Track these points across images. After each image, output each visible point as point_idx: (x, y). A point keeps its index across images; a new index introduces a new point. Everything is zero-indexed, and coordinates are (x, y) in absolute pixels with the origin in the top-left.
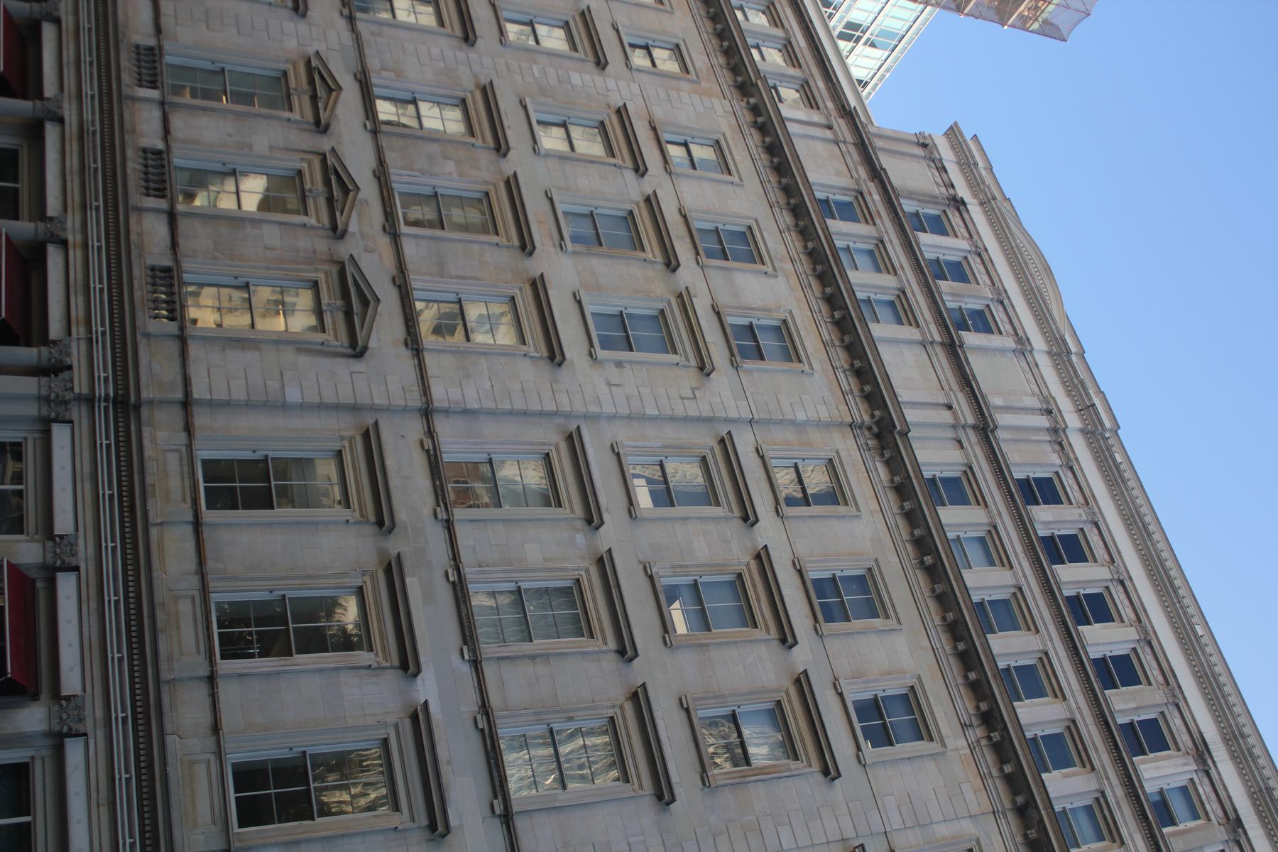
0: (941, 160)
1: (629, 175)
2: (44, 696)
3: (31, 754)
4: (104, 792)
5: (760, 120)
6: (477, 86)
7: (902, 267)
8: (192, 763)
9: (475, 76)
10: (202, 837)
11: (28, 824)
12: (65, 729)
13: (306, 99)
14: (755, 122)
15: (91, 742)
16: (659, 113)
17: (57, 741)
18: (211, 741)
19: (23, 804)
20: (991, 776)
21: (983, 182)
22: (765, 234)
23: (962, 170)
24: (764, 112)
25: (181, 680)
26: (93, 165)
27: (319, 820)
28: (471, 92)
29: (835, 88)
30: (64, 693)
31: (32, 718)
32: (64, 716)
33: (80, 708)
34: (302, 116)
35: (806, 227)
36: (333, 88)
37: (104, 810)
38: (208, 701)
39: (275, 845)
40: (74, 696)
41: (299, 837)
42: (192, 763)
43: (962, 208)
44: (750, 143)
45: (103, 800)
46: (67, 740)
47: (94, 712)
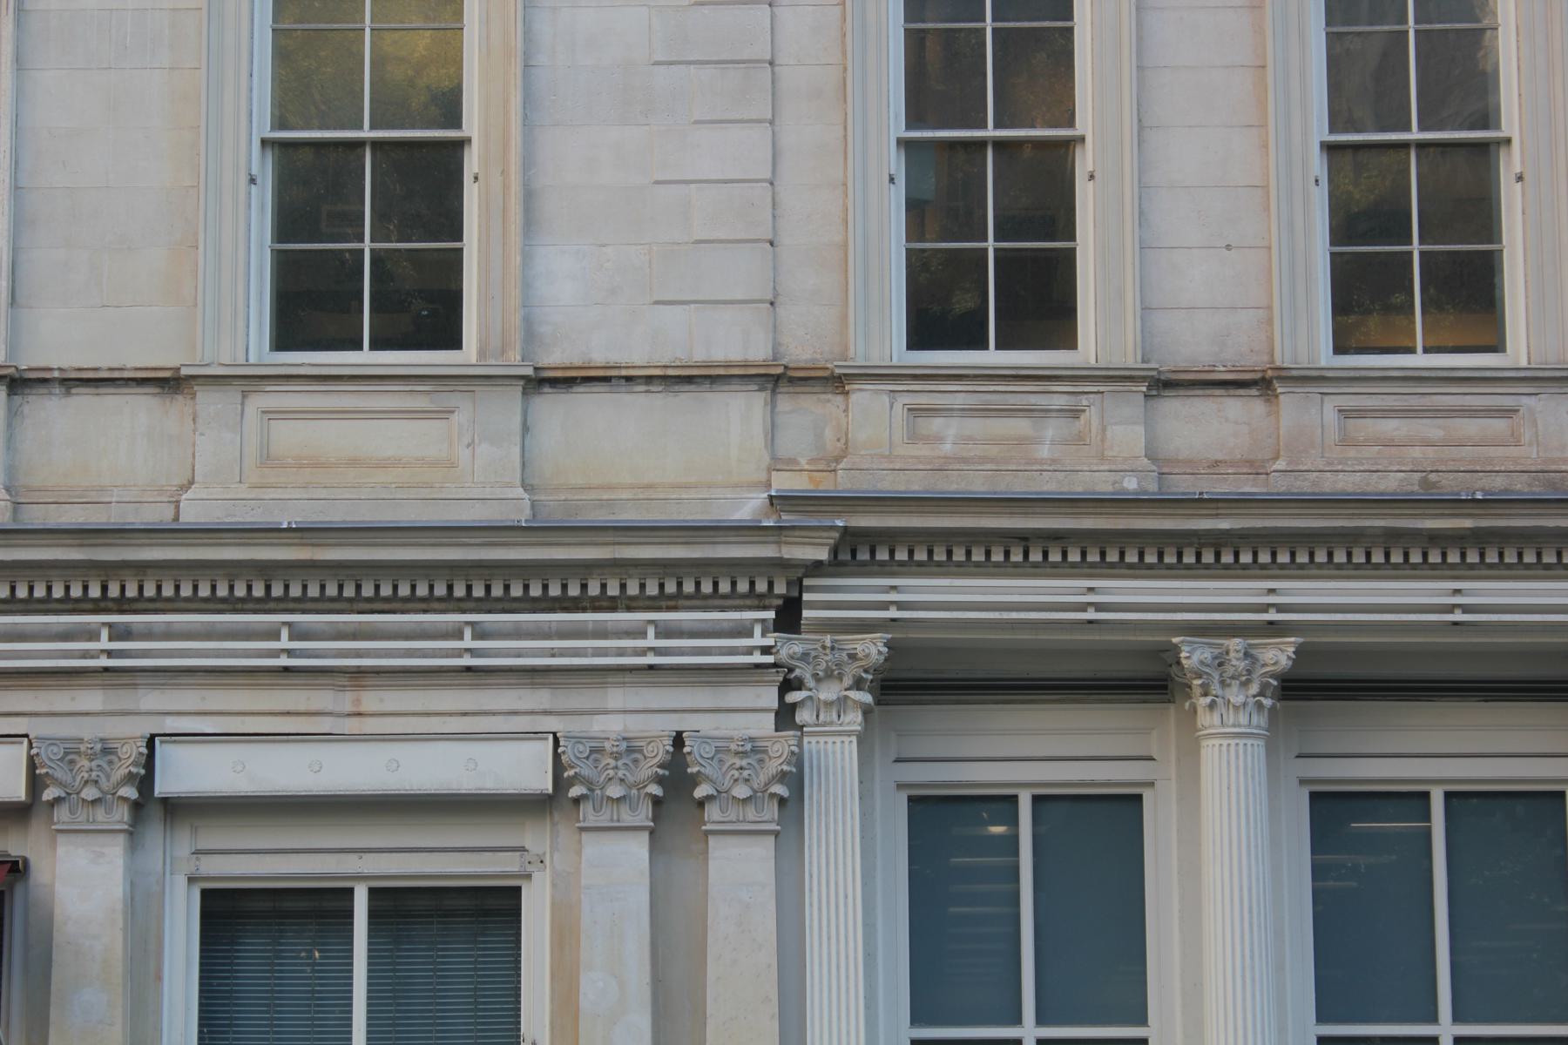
2: (13, 845)
3: (181, 881)
4: (321, 698)
8: (267, 459)
10: (483, 449)
11: (373, 893)
12: (131, 792)
15: (172, 725)
17: (152, 808)
18: (209, 402)
19: (322, 908)
25: (11, 471)
27: (472, 124)
30: (19, 792)
31: (83, 881)
32: (90, 793)
33: (71, 752)
37: (371, 700)
38: (83, 401)
39: (527, 258)
40: (32, 765)
41: (515, 188)
42: (267, 459)
45: (345, 700)
46: (162, 787)
47: (85, 716)
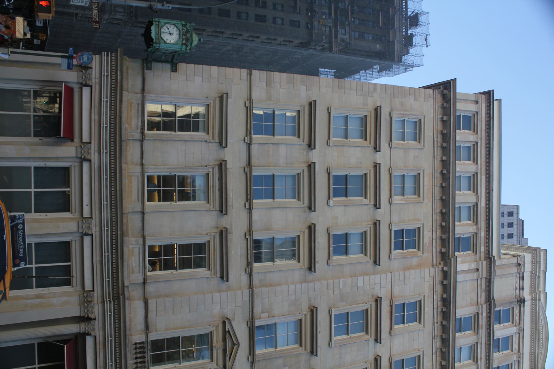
0: (523, 273)
1: (372, 342)
5: (445, 282)
6: (309, 307)
7: (481, 359)
9: (310, 300)
13: (220, 352)
14: (442, 282)
16: (396, 291)
20: (437, 158)
21: (538, 288)
22: (425, 357)
23: (531, 276)
24: (448, 278)
26: (107, 279)
28: (305, 315)
29: (489, 239)
34: (217, 365)
35: (445, 352)
36: (236, 344)
43: (522, 305)
44: (436, 297)
